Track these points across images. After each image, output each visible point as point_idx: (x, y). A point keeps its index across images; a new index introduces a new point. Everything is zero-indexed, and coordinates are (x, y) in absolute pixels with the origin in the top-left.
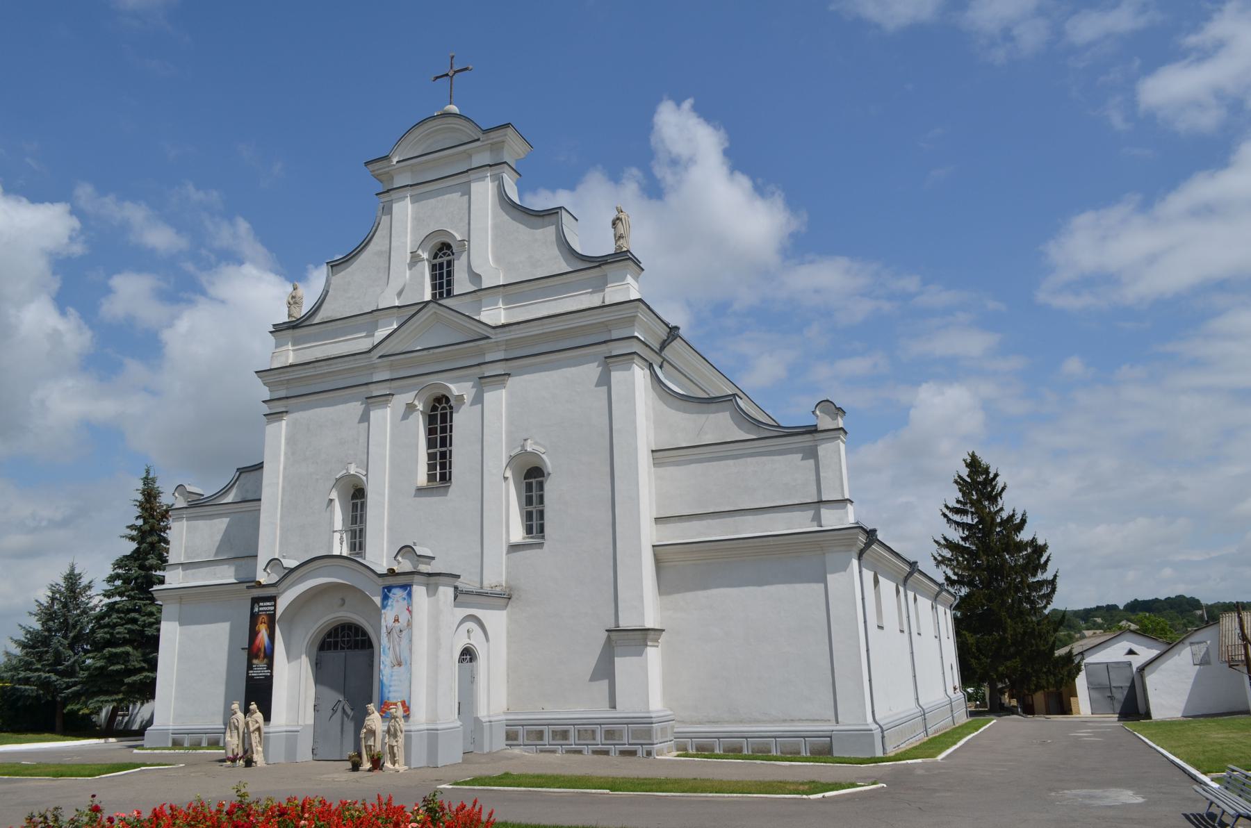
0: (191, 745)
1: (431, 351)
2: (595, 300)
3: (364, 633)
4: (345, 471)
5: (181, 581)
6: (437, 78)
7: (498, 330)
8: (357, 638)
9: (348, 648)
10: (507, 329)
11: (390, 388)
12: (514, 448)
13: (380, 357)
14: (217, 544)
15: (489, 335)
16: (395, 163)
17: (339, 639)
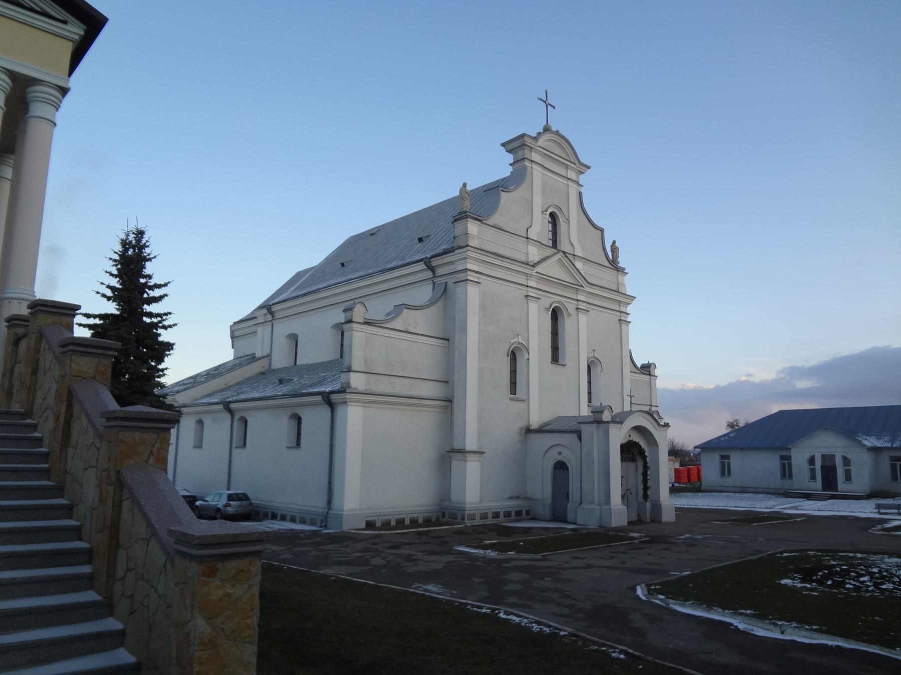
1: (560, 282)
6: (541, 99)
7: (590, 286)
11: (537, 294)
13: (537, 272)
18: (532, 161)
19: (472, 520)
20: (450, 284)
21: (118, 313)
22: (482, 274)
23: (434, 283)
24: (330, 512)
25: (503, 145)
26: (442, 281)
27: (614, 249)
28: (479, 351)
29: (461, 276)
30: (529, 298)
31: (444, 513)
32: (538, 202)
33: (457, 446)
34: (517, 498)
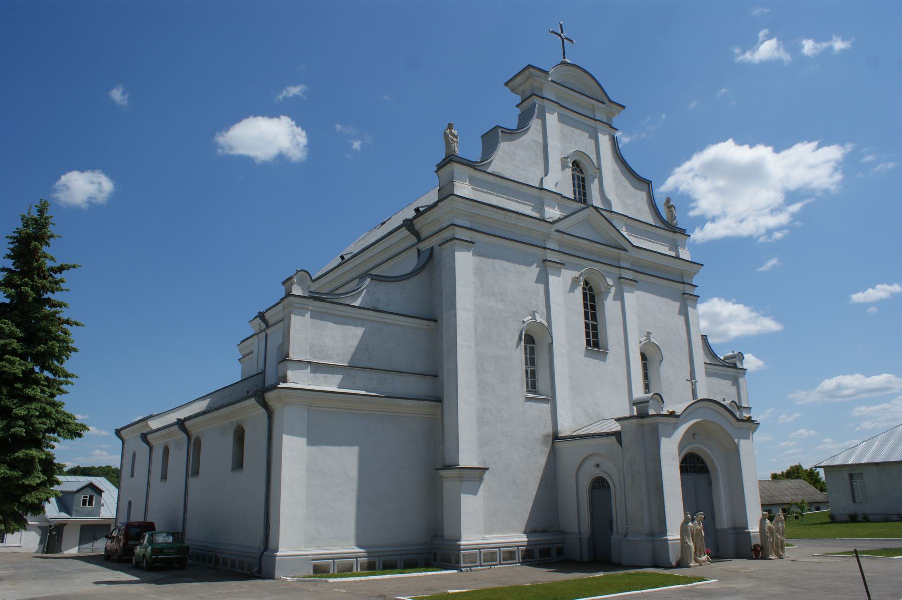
0: (339, 572)
1: (592, 244)
2: (673, 254)
3: (703, 462)
4: (530, 317)
5: (310, 383)
6: (553, 32)
7: (635, 249)
8: (699, 465)
9: (694, 473)
10: (639, 250)
12: (643, 337)
13: (557, 231)
14: (353, 350)
15: (627, 249)
16: (550, 79)
17: (688, 465)
18: (543, 98)
19: (471, 563)
20: (437, 249)
21: (7, 301)
22: (476, 231)
23: (419, 251)
24: (265, 553)
25: (506, 84)
26: (428, 248)
27: (670, 207)
28: (476, 332)
29: (447, 235)
30: (548, 263)
31: (435, 554)
32: (554, 143)
33: (448, 462)
34: (544, 531)
